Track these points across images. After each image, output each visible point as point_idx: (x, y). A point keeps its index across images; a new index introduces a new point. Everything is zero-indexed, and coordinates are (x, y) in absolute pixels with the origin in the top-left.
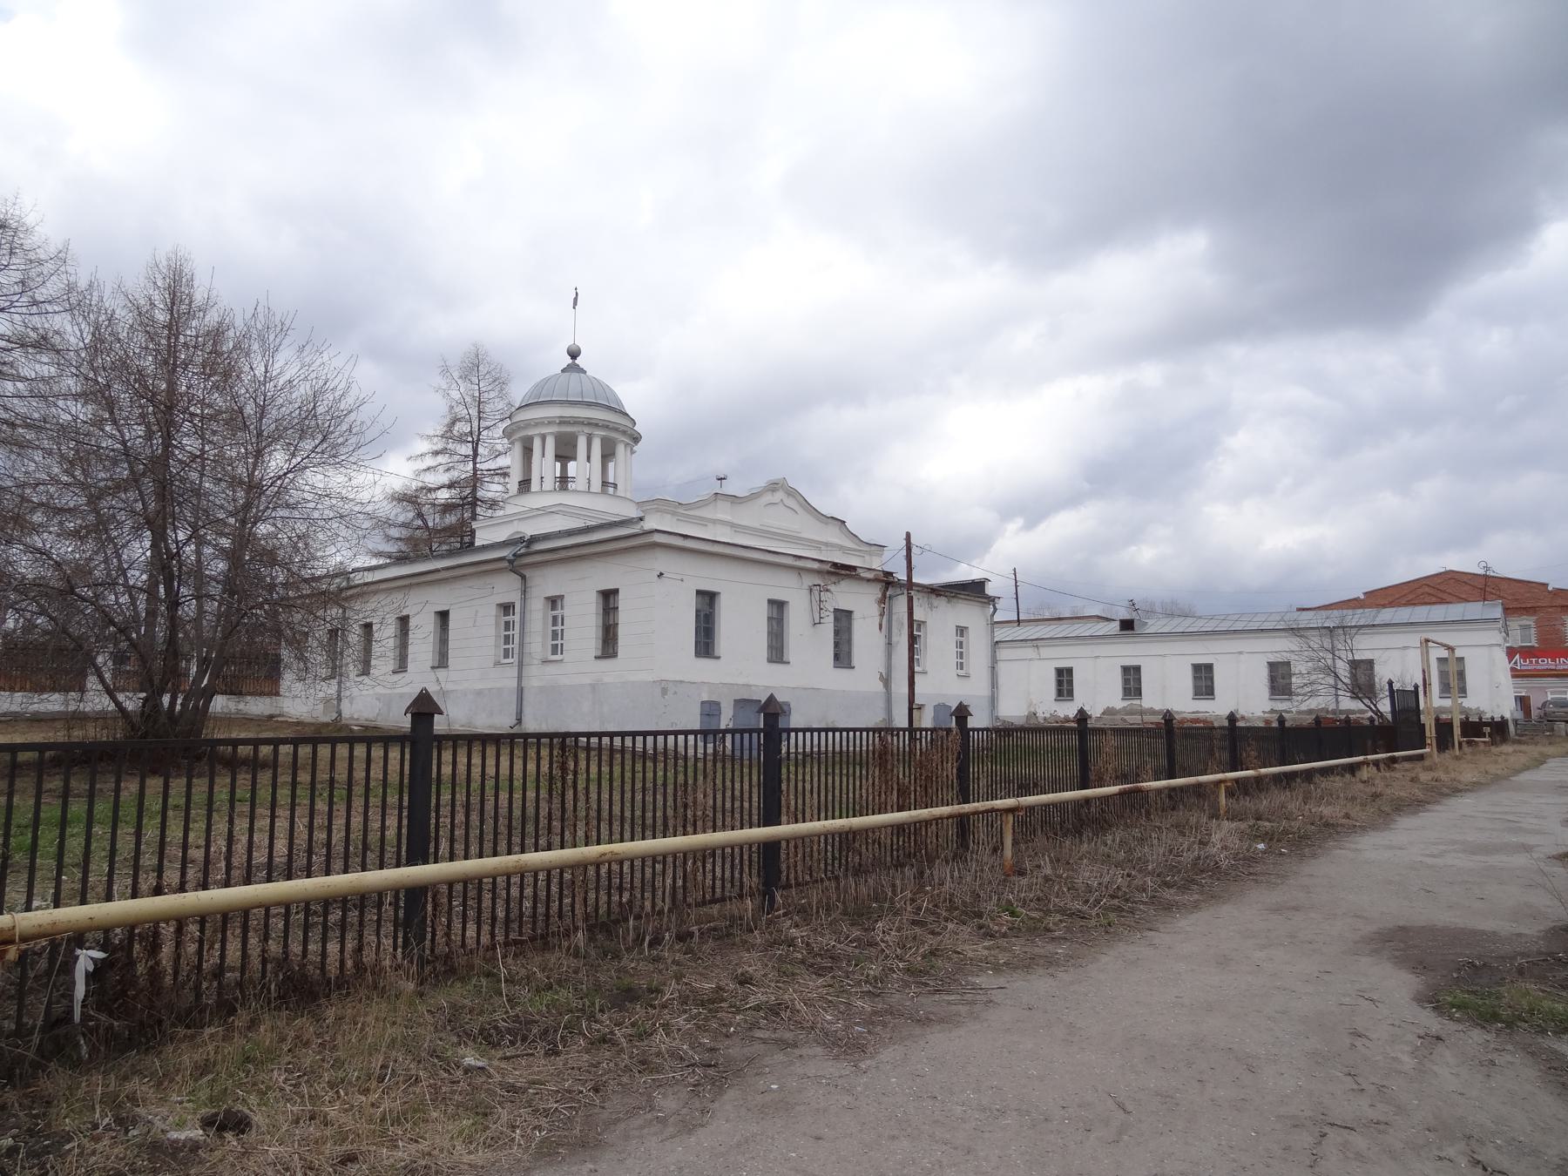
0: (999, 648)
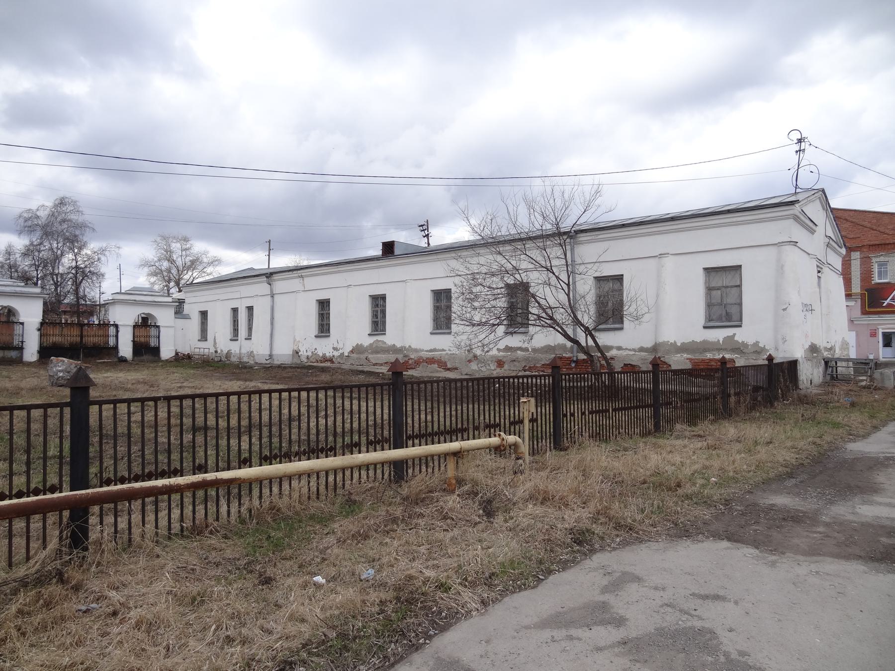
0: (275, 280)
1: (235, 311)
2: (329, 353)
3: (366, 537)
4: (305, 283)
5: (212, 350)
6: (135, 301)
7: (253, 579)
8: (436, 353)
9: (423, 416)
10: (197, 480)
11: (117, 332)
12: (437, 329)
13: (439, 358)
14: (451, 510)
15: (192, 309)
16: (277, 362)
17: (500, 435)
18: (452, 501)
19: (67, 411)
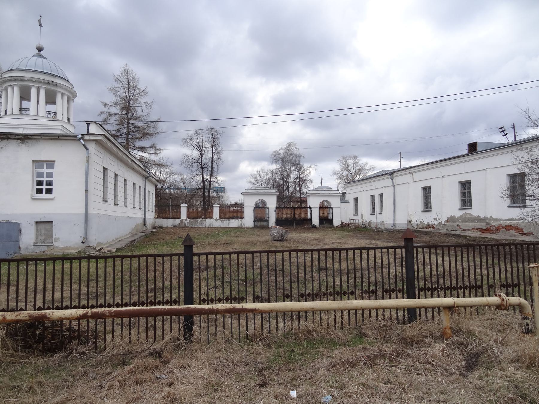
1: (373, 197)
2: (431, 222)
3: (353, 365)
4: (414, 177)
5: (360, 221)
6: (319, 194)
7: (258, 380)
8: (514, 222)
9: (478, 271)
10: (230, 307)
11: (311, 211)
12: (514, 203)
13: (516, 225)
14: (433, 356)
15: (350, 197)
16: (398, 228)
17: (500, 296)
18: (437, 348)
19: (182, 258)
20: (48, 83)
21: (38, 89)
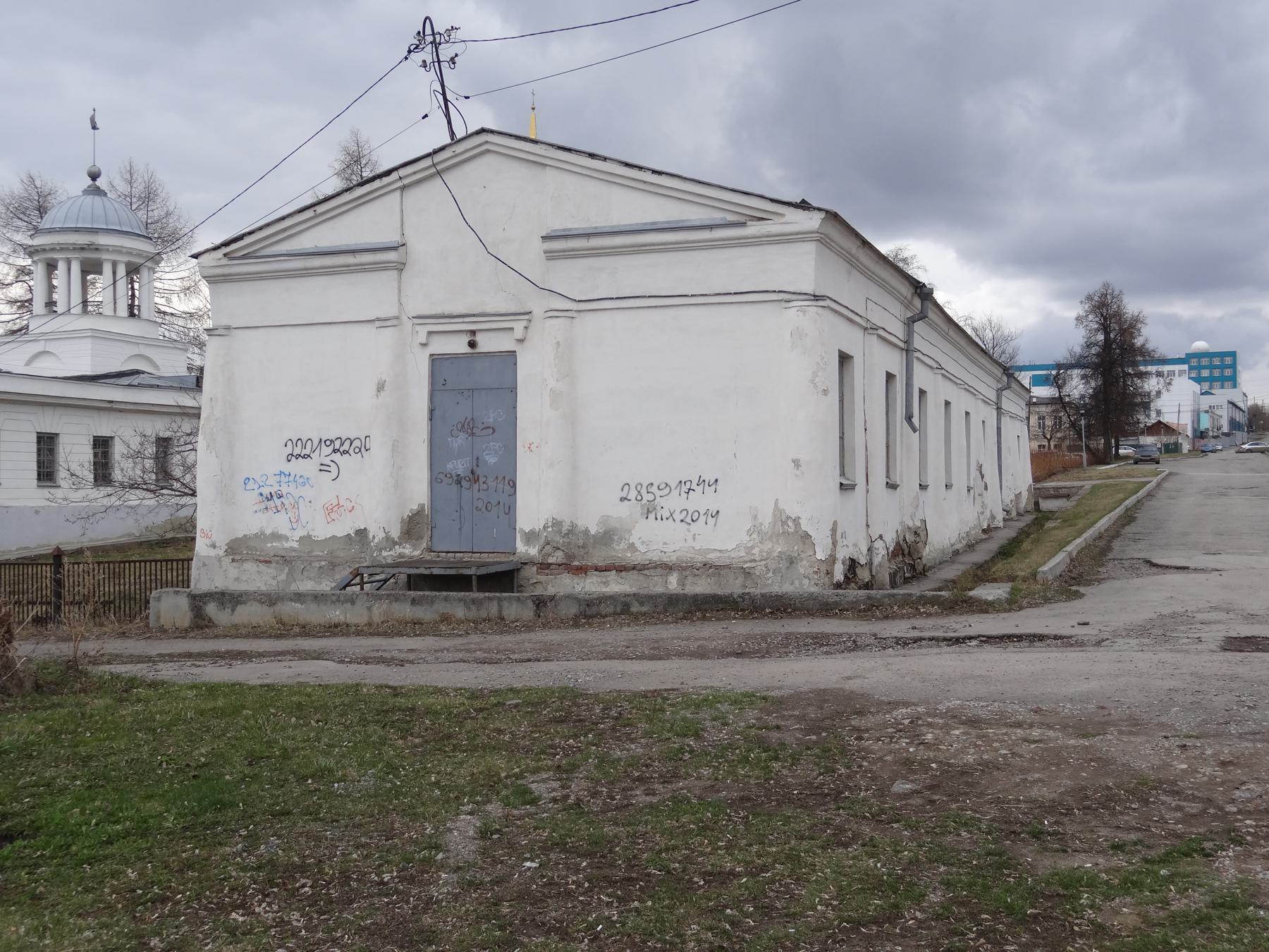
20: (82, 249)
21: (69, 262)
